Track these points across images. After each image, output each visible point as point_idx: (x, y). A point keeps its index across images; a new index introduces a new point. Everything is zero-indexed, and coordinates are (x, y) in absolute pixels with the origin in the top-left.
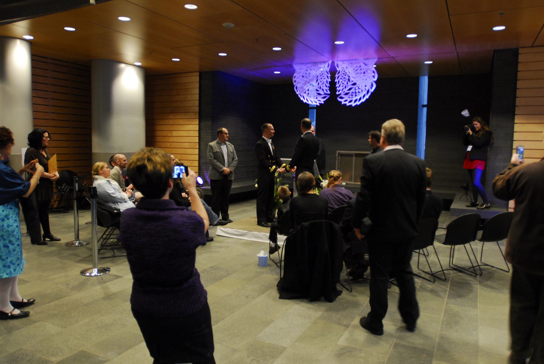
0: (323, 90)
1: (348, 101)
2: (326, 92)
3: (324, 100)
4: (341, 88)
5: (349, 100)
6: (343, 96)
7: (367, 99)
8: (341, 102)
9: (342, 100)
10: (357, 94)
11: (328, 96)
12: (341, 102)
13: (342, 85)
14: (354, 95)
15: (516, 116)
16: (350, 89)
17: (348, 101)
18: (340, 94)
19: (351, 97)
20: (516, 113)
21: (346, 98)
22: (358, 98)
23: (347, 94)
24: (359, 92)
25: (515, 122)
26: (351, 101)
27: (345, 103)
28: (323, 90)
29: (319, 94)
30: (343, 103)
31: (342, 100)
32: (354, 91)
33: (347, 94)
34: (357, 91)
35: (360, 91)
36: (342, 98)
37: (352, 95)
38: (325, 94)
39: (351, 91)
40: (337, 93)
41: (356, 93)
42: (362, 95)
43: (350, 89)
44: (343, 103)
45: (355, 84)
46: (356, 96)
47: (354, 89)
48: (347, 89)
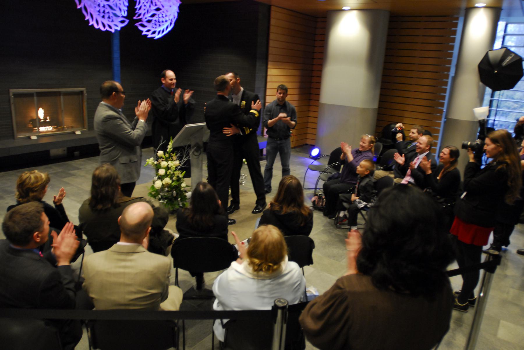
0: (120, 10)
1: (151, 32)
2: (123, 15)
3: (123, 25)
4: (142, 11)
5: (153, 30)
6: (146, 24)
7: (169, 32)
8: (142, 31)
9: (144, 30)
10: (161, 24)
11: (127, 21)
12: (142, 31)
13: (143, 7)
14: (158, 24)
15: (269, 63)
16: (153, 16)
17: (151, 32)
18: (140, 20)
19: (155, 26)
20: (270, 59)
21: (149, 26)
22: (161, 29)
23: (149, 21)
24: (163, 22)
25: (269, 66)
26: (154, 33)
27: (147, 33)
28: (120, 10)
29: (115, 15)
30: (143, 34)
31: (144, 30)
32: (157, 19)
33: (149, 21)
34: (161, 20)
35: (164, 20)
36: (144, 26)
37: (155, 25)
38: (123, 17)
39: (154, 19)
40: (135, 18)
41: (159, 22)
42: (165, 27)
43: (153, 16)
44: (143, 34)
45: (158, 9)
46: (160, 26)
47: (157, 16)
48: (150, 14)
